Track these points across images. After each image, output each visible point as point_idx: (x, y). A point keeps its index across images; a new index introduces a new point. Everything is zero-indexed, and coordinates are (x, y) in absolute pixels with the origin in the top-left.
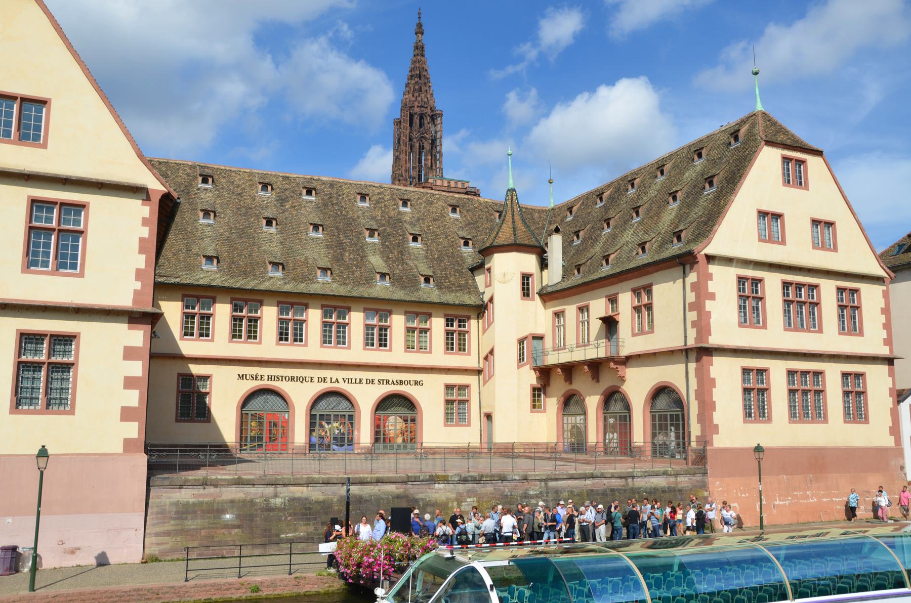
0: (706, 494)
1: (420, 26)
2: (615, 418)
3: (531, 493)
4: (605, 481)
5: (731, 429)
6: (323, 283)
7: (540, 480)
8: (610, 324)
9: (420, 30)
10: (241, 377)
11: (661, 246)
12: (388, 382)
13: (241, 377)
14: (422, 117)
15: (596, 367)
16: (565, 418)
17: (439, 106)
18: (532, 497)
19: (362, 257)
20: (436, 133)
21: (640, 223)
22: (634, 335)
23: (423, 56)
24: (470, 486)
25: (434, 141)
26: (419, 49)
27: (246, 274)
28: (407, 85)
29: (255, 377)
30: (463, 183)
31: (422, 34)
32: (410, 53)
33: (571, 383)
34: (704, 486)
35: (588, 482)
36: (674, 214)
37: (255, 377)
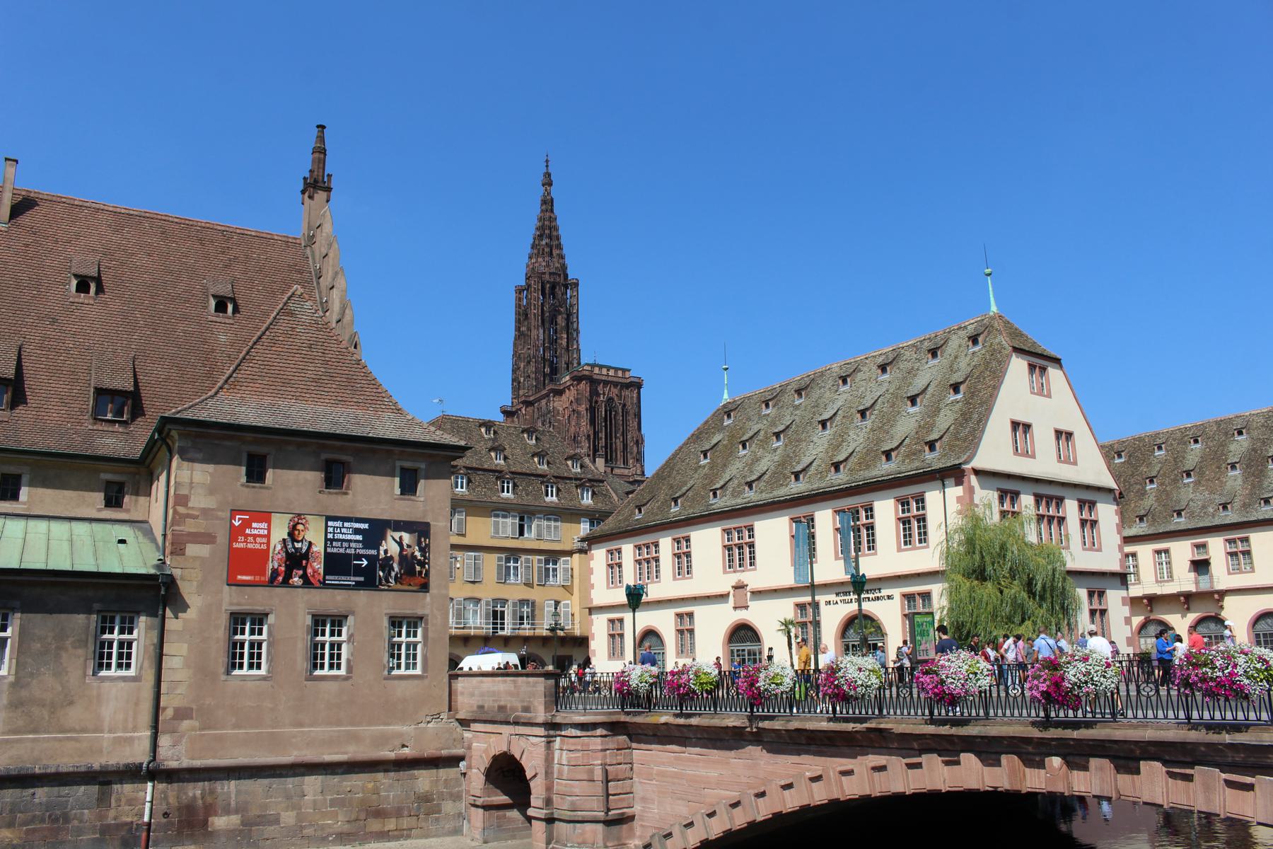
1: (548, 175)
2: (1210, 637)
8: (1201, 566)
9: (548, 183)
11: (1245, 506)
14: (553, 287)
15: (1186, 600)
16: (1142, 641)
17: (572, 274)
20: (571, 305)
21: (1197, 483)
22: (1229, 573)
23: (552, 211)
25: (569, 315)
26: (548, 203)
28: (533, 247)
30: (624, 370)
31: (550, 184)
32: (536, 210)
33: (1151, 611)
36: (1240, 481)
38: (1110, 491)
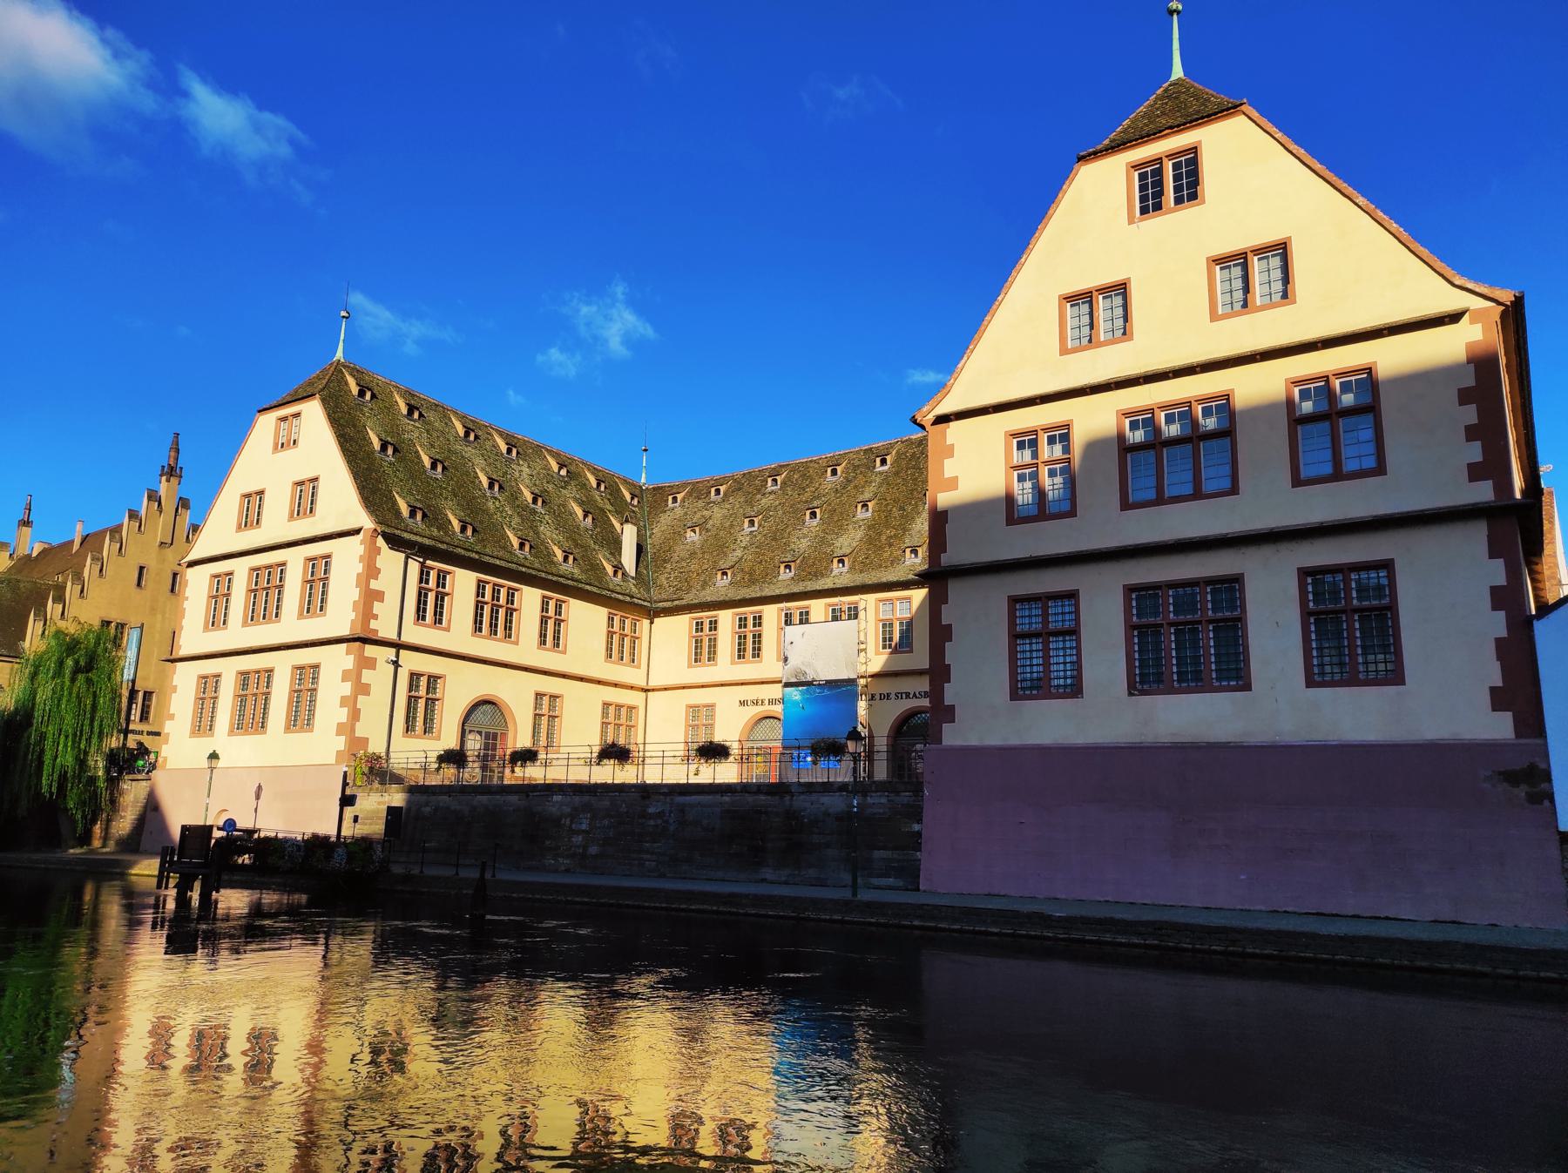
0: (916, 827)
3: (651, 810)
4: (750, 798)
5: (987, 715)
6: (840, 574)
7: (664, 794)
10: (743, 703)
12: (908, 695)
13: (743, 703)
18: (651, 816)
19: (905, 530)
24: (586, 798)
27: (753, 582)
29: (755, 703)
34: (916, 814)
35: (726, 799)
37: (755, 703)
38: (357, 532)
